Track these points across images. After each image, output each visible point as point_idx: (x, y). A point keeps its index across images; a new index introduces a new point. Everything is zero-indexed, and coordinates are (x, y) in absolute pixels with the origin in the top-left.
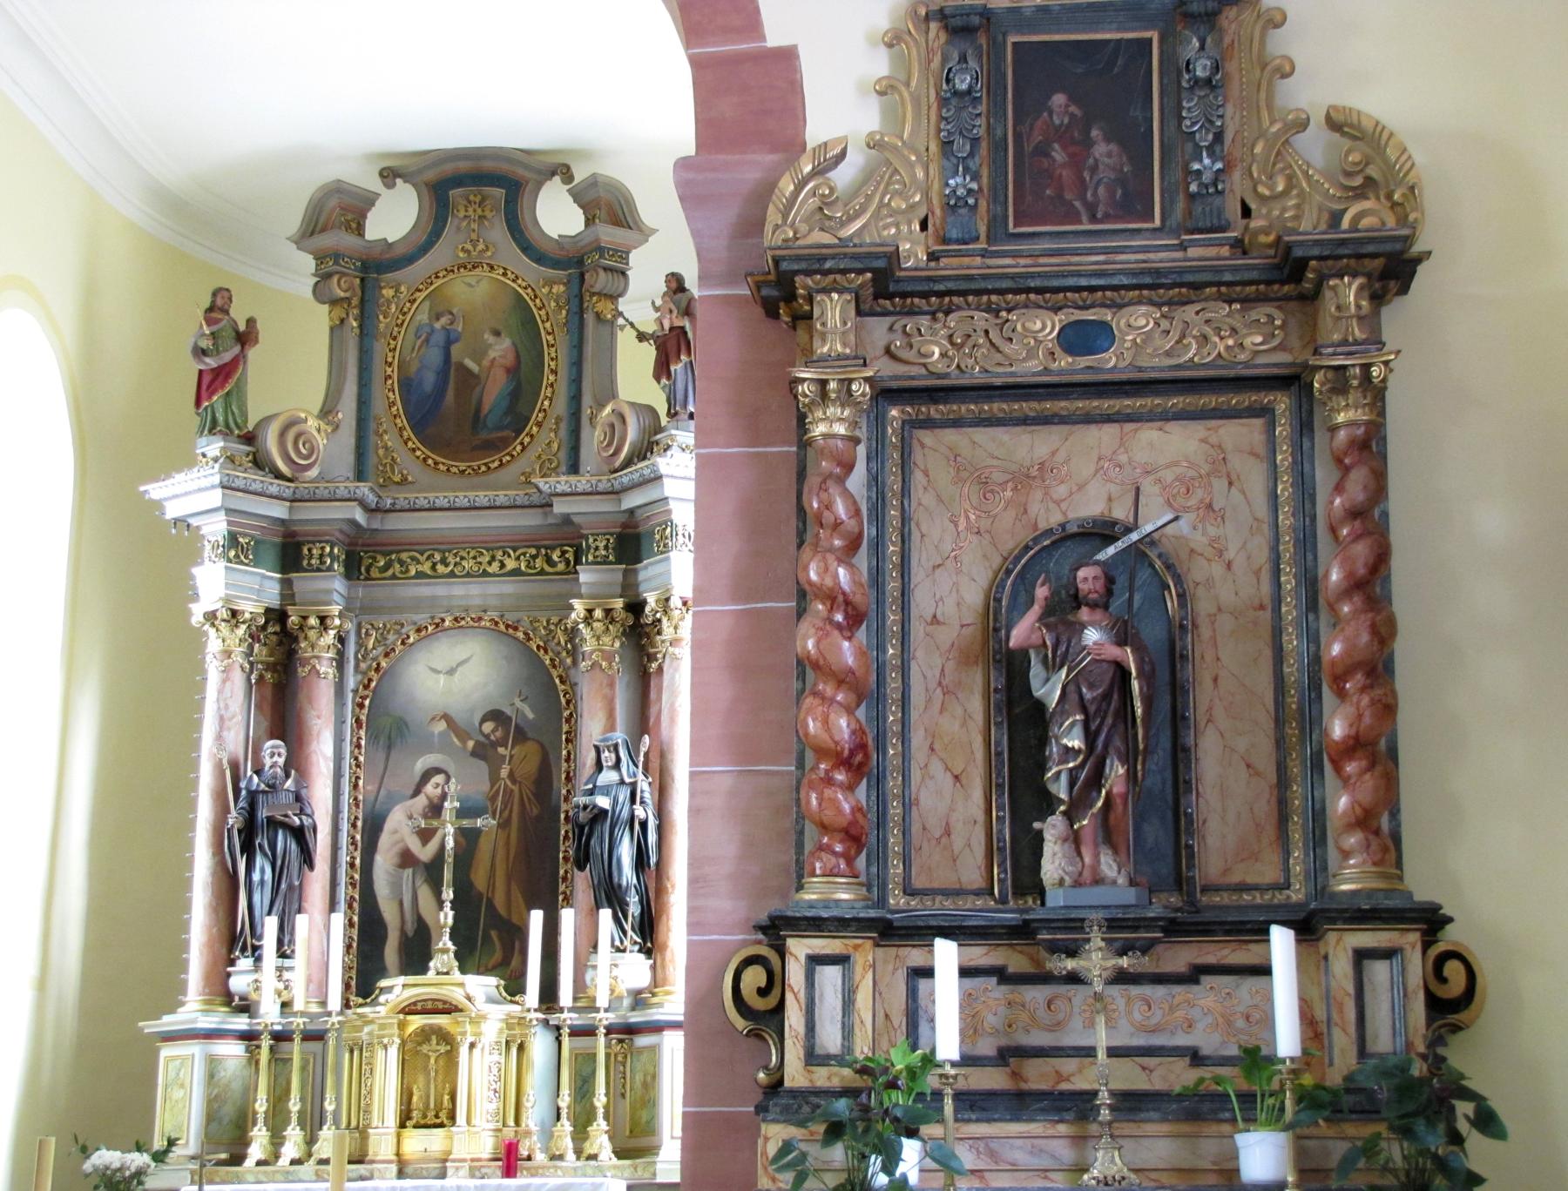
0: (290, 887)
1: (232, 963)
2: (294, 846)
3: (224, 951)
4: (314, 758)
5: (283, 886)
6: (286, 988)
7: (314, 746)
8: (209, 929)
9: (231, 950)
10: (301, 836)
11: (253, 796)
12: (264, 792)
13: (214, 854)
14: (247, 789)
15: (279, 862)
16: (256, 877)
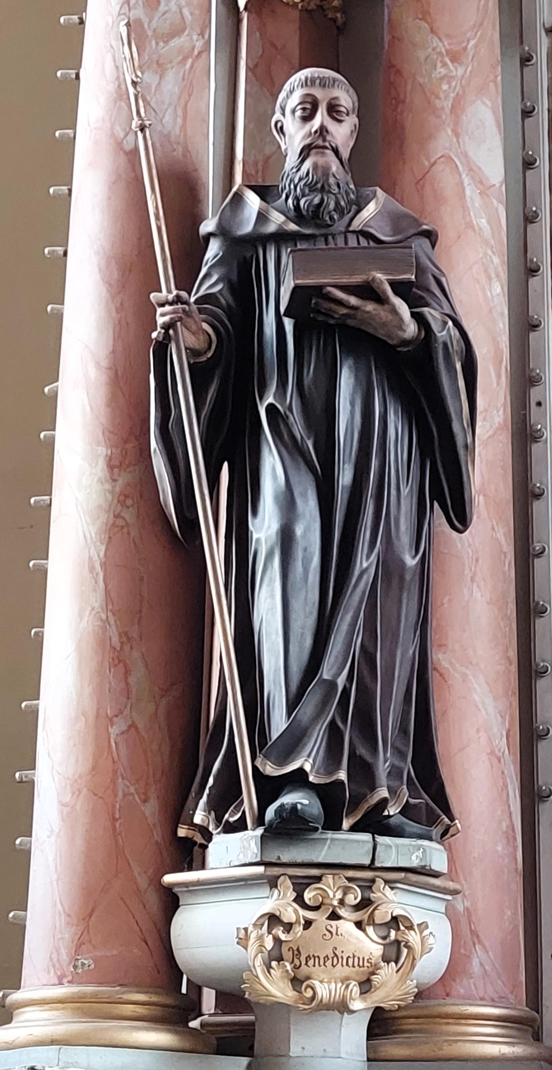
0: (389, 568)
1: (190, 854)
2: (396, 425)
3: (151, 810)
4: (445, 179)
5: (365, 563)
6: (394, 952)
7: (443, 143)
8: (102, 721)
9: (178, 811)
10: (420, 377)
11: (244, 254)
12: (281, 238)
13: (112, 466)
14: (223, 232)
15: (345, 477)
16: (264, 528)
